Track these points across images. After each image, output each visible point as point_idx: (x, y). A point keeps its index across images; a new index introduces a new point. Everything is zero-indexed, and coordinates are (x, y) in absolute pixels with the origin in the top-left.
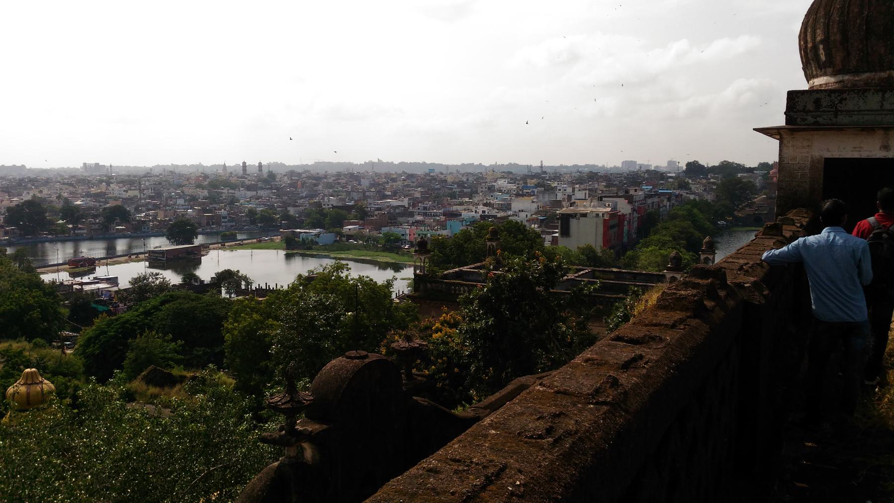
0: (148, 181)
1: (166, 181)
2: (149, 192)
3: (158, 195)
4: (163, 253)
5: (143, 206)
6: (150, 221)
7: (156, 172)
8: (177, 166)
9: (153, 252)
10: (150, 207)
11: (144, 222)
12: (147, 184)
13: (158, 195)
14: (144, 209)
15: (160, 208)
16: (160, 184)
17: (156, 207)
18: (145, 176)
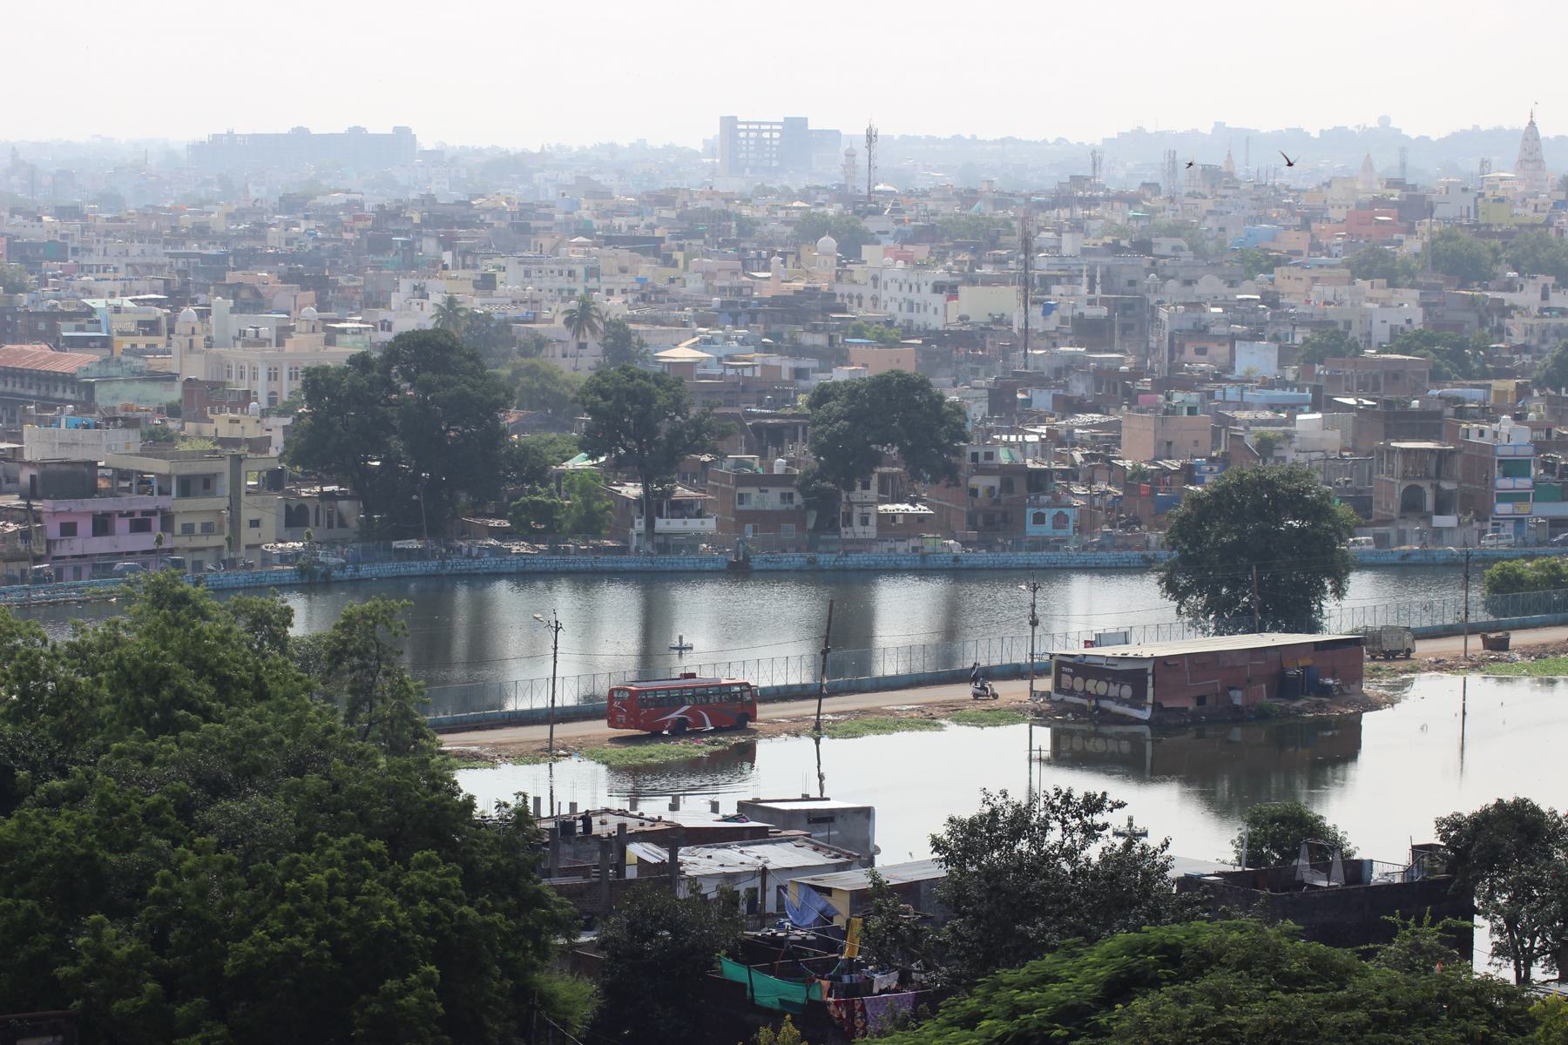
0: (1078, 227)
1: (1173, 231)
2: (1075, 299)
3: (1128, 316)
4: (1133, 675)
5: (1039, 381)
6: (1071, 475)
7: (1120, 175)
8: (1248, 138)
9: (1081, 668)
10: (1079, 388)
11: (1037, 481)
12: (1069, 244)
13: (1128, 316)
14: (1042, 399)
15: (1131, 397)
16: (1143, 247)
17: (1114, 390)
18: (1061, 199)
